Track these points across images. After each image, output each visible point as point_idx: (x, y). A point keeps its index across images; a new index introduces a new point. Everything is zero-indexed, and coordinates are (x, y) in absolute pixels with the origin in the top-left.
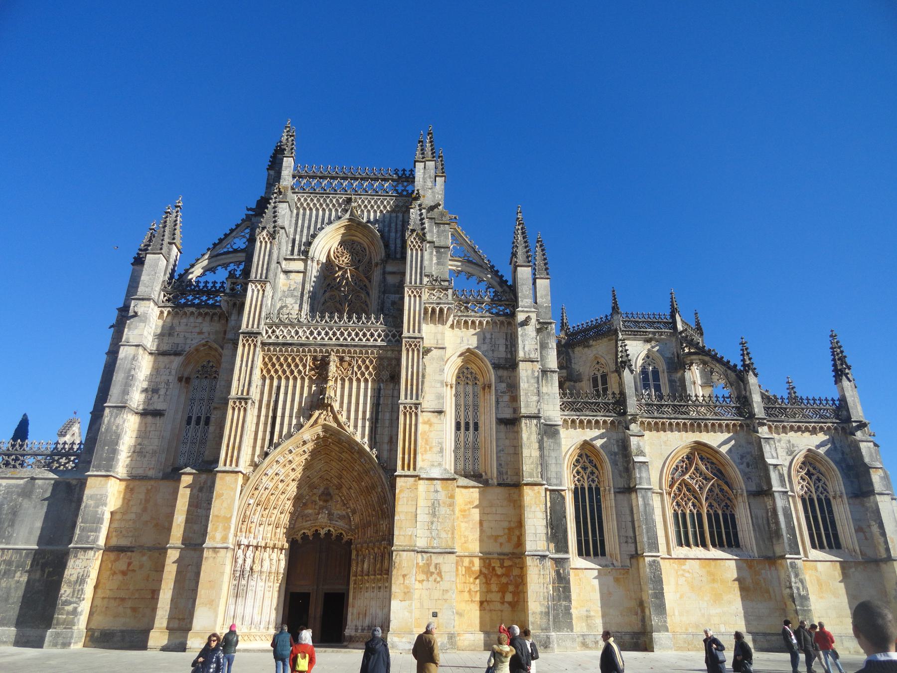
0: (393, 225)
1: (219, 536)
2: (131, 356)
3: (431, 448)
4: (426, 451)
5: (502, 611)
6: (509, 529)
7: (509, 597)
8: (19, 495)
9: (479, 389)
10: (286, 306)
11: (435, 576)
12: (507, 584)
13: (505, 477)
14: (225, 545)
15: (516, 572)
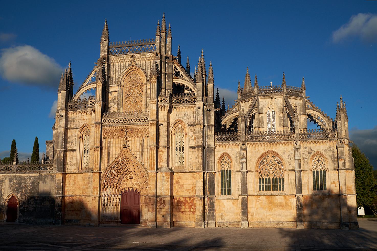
0: (149, 66)
1: (95, 193)
2: (62, 132)
3: (163, 160)
4: (161, 162)
5: (190, 214)
6: (192, 187)
7: (192, 210)
8: (38, 179)
9: (184, 134)
10: (112, 107)
11: (163, 204)
12: (192, 205)
13: (192, 169)
14: (98, 196)
15: (194, 202)
